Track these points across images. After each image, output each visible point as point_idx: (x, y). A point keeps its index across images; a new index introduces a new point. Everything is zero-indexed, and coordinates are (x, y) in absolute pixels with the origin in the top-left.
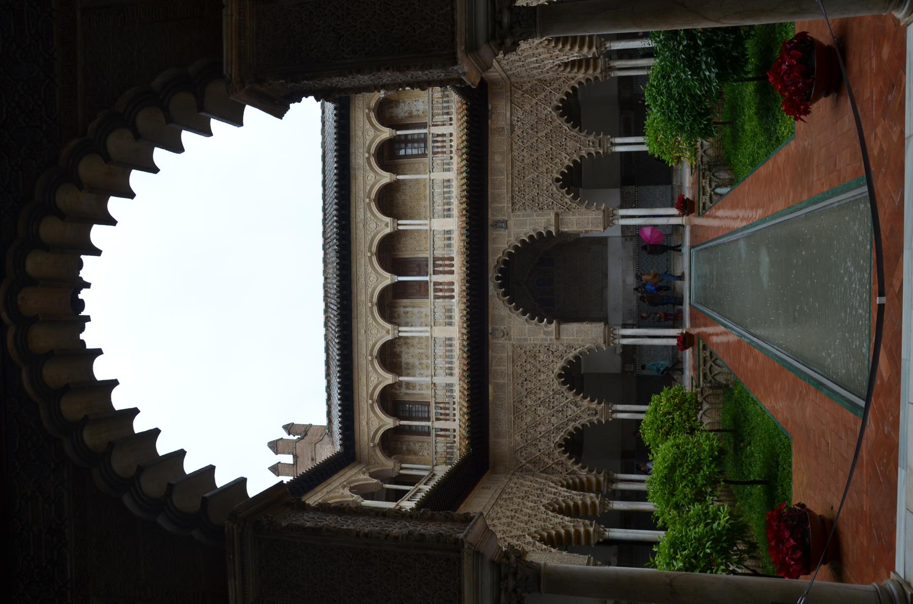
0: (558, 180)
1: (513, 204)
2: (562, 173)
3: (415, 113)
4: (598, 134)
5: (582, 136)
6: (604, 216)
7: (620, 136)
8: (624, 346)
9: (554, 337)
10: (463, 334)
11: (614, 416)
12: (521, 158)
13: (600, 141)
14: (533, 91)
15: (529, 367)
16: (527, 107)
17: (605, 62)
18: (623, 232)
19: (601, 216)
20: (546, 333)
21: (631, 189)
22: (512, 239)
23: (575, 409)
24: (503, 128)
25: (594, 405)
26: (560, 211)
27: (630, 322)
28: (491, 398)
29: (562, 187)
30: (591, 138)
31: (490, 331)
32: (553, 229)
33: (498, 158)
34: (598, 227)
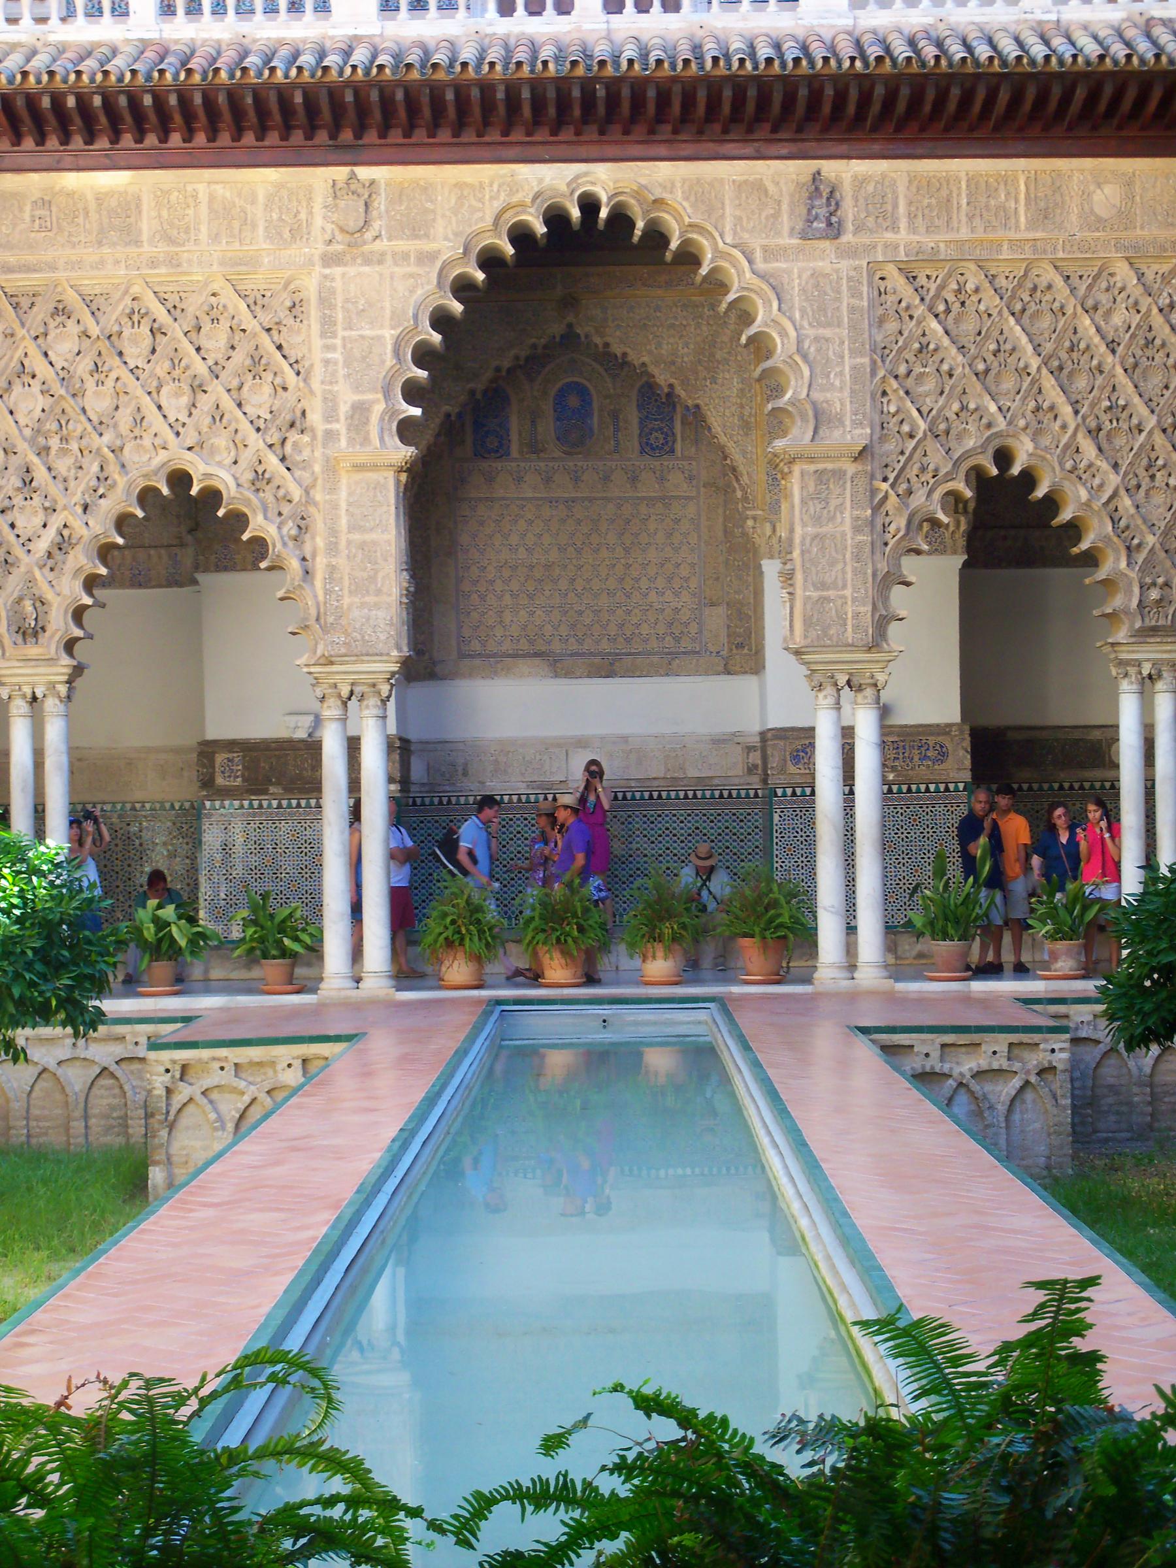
0: (1003, 457)
2: (1028, 479)
8: (313, 748)
10: (347, 53)
11: (19, 707)
12: (1104, 298)
15: (216, 341)
19: (849, 635)
20: (360, 411)
21: (958, 766)
23: (42, 546)
25: (59, 624)
27: (418, 771)
28: (72, 180)
29: (977, 476)
31: (364, 173)
34: (808, 623)
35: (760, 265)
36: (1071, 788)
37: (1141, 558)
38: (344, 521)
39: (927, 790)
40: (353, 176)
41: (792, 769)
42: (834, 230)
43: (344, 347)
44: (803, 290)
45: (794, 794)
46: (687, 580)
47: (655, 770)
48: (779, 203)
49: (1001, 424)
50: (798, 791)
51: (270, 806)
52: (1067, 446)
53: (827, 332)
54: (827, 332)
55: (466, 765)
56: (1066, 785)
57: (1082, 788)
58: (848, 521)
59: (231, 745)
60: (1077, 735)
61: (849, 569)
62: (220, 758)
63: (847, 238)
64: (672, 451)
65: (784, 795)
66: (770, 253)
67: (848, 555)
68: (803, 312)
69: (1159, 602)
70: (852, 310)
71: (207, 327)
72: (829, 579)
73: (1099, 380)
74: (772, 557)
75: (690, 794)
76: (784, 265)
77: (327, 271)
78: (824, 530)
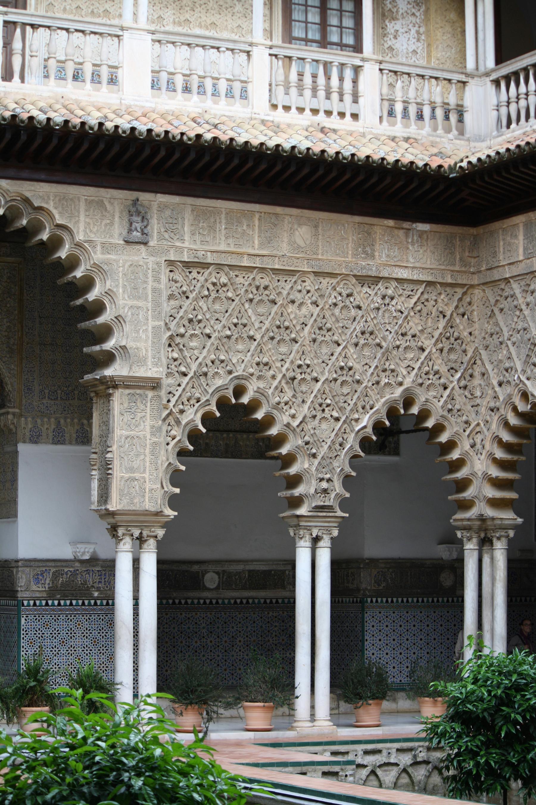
1: (187, 265)
3: (391, 27)
4: (344, 504)
5: (342, 464)
6: (147, 513)
13: (330, 508)
14: (450, 342)
16: (414, 325)
17: (505, 528)
18: (30, 563)
22: (98, 256)
24: (373, 257)
26: (163, 393)
29: (222, 403)
30: (338, 487)
33: (303, 234)
34: (122, 495)
36: (180, 603)
37: (316, 462)
41: (34, 588)
45: (35, 605)
49: (239, 371)
50: (38, 603)
52: (276, 388)
53: (140, 303)
54: (140, 303)
56: (177, 601)
57: (186, 603)
58: (148, 428)
60: (184, 567)
61: (148, 459)
65: (29, 605)
66: (107, 248)
67: (147, 451)
69: (325, 491)
70: (154, 290)
72: (135, 464)
73: (296, 347)
74: (24, 442)
78: (132, 433)
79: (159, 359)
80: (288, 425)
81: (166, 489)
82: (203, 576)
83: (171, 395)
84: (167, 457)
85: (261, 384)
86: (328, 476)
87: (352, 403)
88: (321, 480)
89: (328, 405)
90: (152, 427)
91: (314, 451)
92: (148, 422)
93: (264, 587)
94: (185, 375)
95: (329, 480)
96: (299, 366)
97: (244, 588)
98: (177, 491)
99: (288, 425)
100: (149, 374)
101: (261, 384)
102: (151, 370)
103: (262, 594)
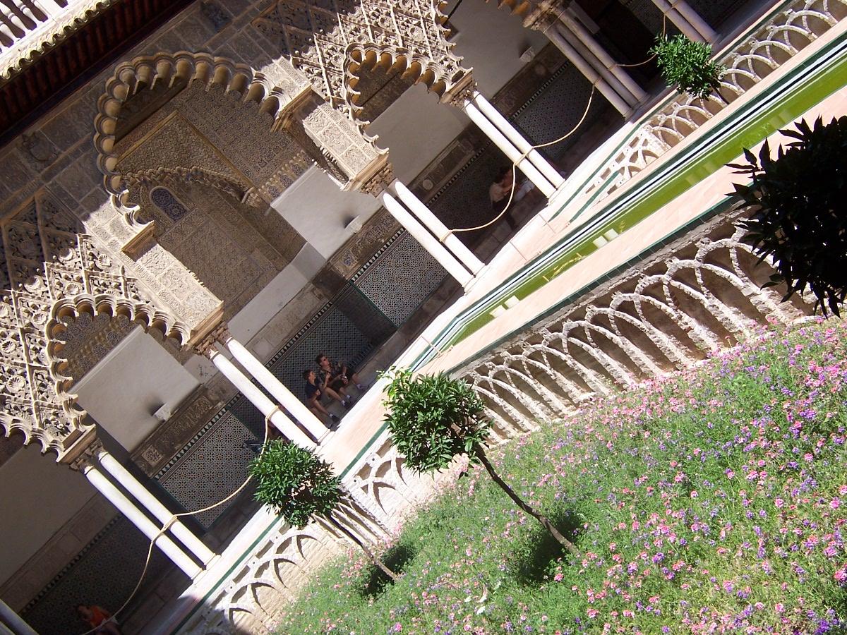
5: (443, 43)
7: (491, 102)
9: (122, 245)
18: (335, 255)
20: (115, 226)
31: (29, 132)
32: (284, 102)
35: (214, 52)
38: (149, 272)
39: (399, 235)
40: (24, 137)
41: (350, 267)
42: (227, 19)
43: (85, 206)
44: (238, 51)
45: (359, 275)
46: (234, 251)
47: (288, 328)
48: (199, 24)
50: (359, 273)
51: (182, 455)
55: (221, 388)
59: (143, 444)
61: (346, 134)
62: (145, 456)
63: (235, 19)
64: (185, 211)
65: (356, 279)
67: (342, 131)
68: (244, 57)
69: (449, 67)
70: (260, 44)
71: (21, 246)
74: (272, 201)
75: (285, 348)
76: (222, 46)
77: (51, 182)
79: (300, 77)
80: (398, 50)
81: (370, 141)
82: (422, 186)
83: (324, 91)
84: (354, 125)
85: (363, 42)
86: (443, 57)
87: (418, 9)
88: (442, 62)
89: (408, 21)
90: (332, 116)
91: (423, 51)
92: (327, 115)
93: (456, 164)
94: (320, 74)
95: (446, 59)
96: (373, 14)
97: (447, 173)
98: (377, 137)
99: (398, 50)
100: (302, 90)
101: (363, 42)
102: (301, 87)
103: (458, 168)
